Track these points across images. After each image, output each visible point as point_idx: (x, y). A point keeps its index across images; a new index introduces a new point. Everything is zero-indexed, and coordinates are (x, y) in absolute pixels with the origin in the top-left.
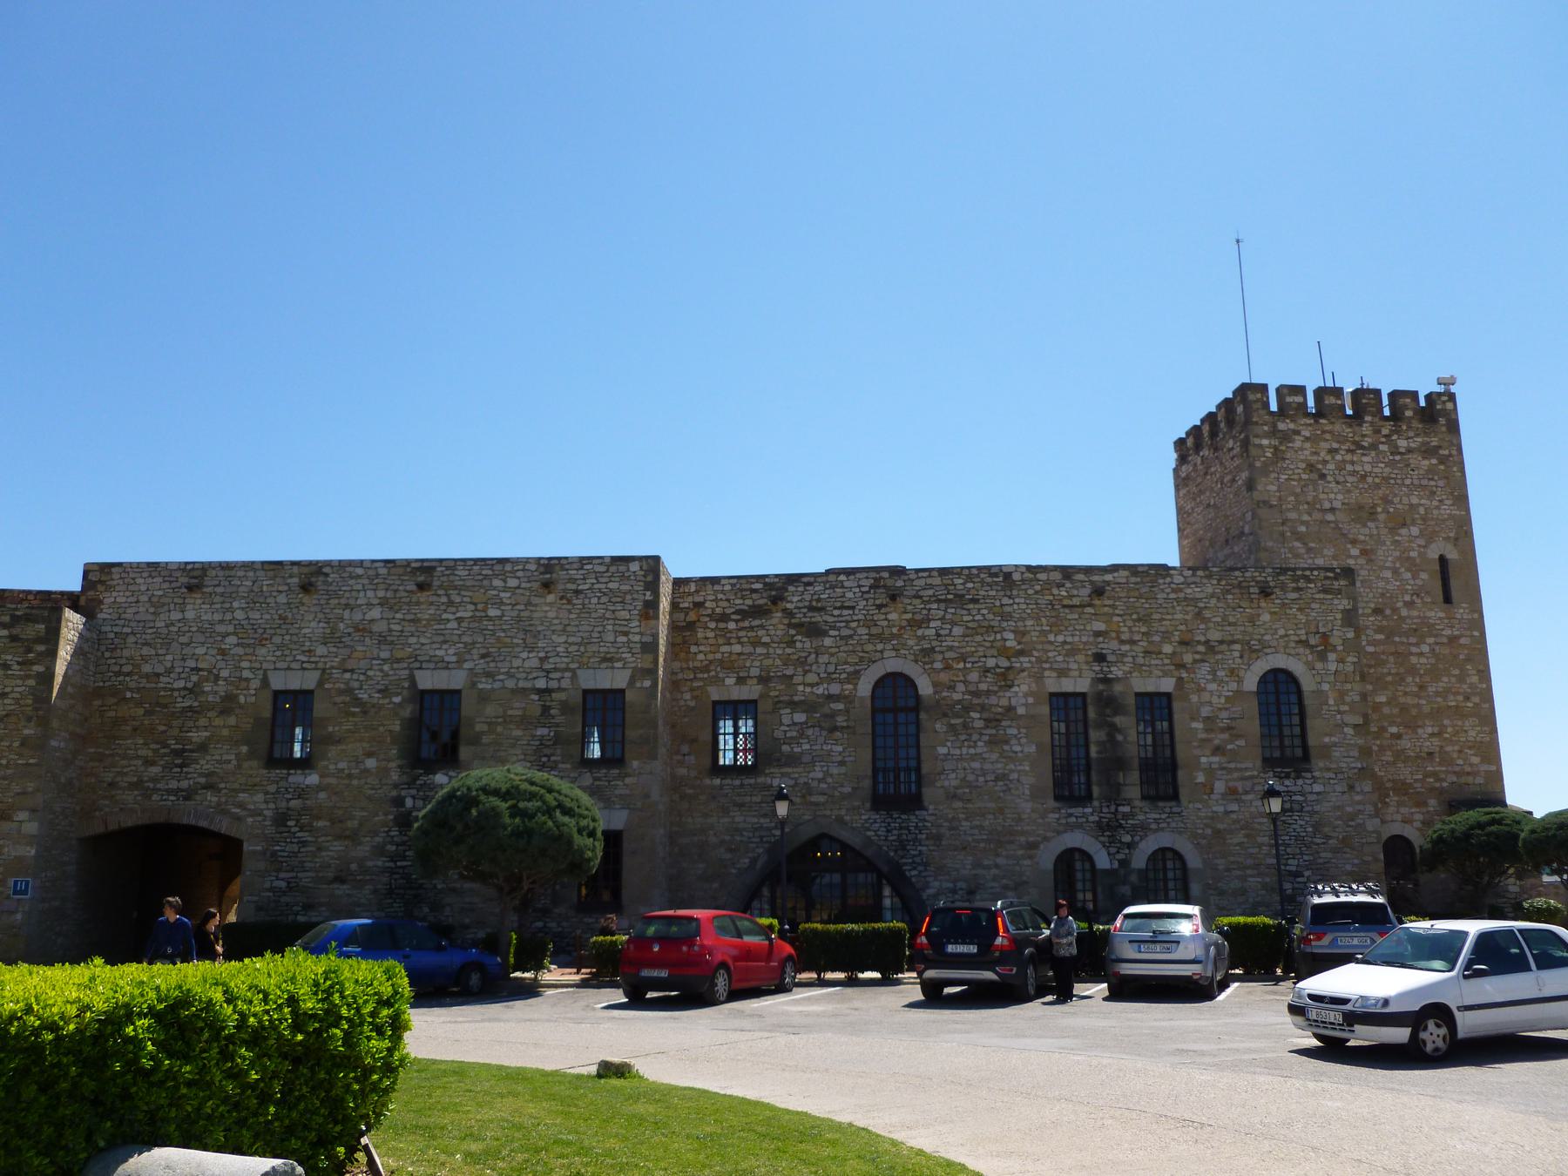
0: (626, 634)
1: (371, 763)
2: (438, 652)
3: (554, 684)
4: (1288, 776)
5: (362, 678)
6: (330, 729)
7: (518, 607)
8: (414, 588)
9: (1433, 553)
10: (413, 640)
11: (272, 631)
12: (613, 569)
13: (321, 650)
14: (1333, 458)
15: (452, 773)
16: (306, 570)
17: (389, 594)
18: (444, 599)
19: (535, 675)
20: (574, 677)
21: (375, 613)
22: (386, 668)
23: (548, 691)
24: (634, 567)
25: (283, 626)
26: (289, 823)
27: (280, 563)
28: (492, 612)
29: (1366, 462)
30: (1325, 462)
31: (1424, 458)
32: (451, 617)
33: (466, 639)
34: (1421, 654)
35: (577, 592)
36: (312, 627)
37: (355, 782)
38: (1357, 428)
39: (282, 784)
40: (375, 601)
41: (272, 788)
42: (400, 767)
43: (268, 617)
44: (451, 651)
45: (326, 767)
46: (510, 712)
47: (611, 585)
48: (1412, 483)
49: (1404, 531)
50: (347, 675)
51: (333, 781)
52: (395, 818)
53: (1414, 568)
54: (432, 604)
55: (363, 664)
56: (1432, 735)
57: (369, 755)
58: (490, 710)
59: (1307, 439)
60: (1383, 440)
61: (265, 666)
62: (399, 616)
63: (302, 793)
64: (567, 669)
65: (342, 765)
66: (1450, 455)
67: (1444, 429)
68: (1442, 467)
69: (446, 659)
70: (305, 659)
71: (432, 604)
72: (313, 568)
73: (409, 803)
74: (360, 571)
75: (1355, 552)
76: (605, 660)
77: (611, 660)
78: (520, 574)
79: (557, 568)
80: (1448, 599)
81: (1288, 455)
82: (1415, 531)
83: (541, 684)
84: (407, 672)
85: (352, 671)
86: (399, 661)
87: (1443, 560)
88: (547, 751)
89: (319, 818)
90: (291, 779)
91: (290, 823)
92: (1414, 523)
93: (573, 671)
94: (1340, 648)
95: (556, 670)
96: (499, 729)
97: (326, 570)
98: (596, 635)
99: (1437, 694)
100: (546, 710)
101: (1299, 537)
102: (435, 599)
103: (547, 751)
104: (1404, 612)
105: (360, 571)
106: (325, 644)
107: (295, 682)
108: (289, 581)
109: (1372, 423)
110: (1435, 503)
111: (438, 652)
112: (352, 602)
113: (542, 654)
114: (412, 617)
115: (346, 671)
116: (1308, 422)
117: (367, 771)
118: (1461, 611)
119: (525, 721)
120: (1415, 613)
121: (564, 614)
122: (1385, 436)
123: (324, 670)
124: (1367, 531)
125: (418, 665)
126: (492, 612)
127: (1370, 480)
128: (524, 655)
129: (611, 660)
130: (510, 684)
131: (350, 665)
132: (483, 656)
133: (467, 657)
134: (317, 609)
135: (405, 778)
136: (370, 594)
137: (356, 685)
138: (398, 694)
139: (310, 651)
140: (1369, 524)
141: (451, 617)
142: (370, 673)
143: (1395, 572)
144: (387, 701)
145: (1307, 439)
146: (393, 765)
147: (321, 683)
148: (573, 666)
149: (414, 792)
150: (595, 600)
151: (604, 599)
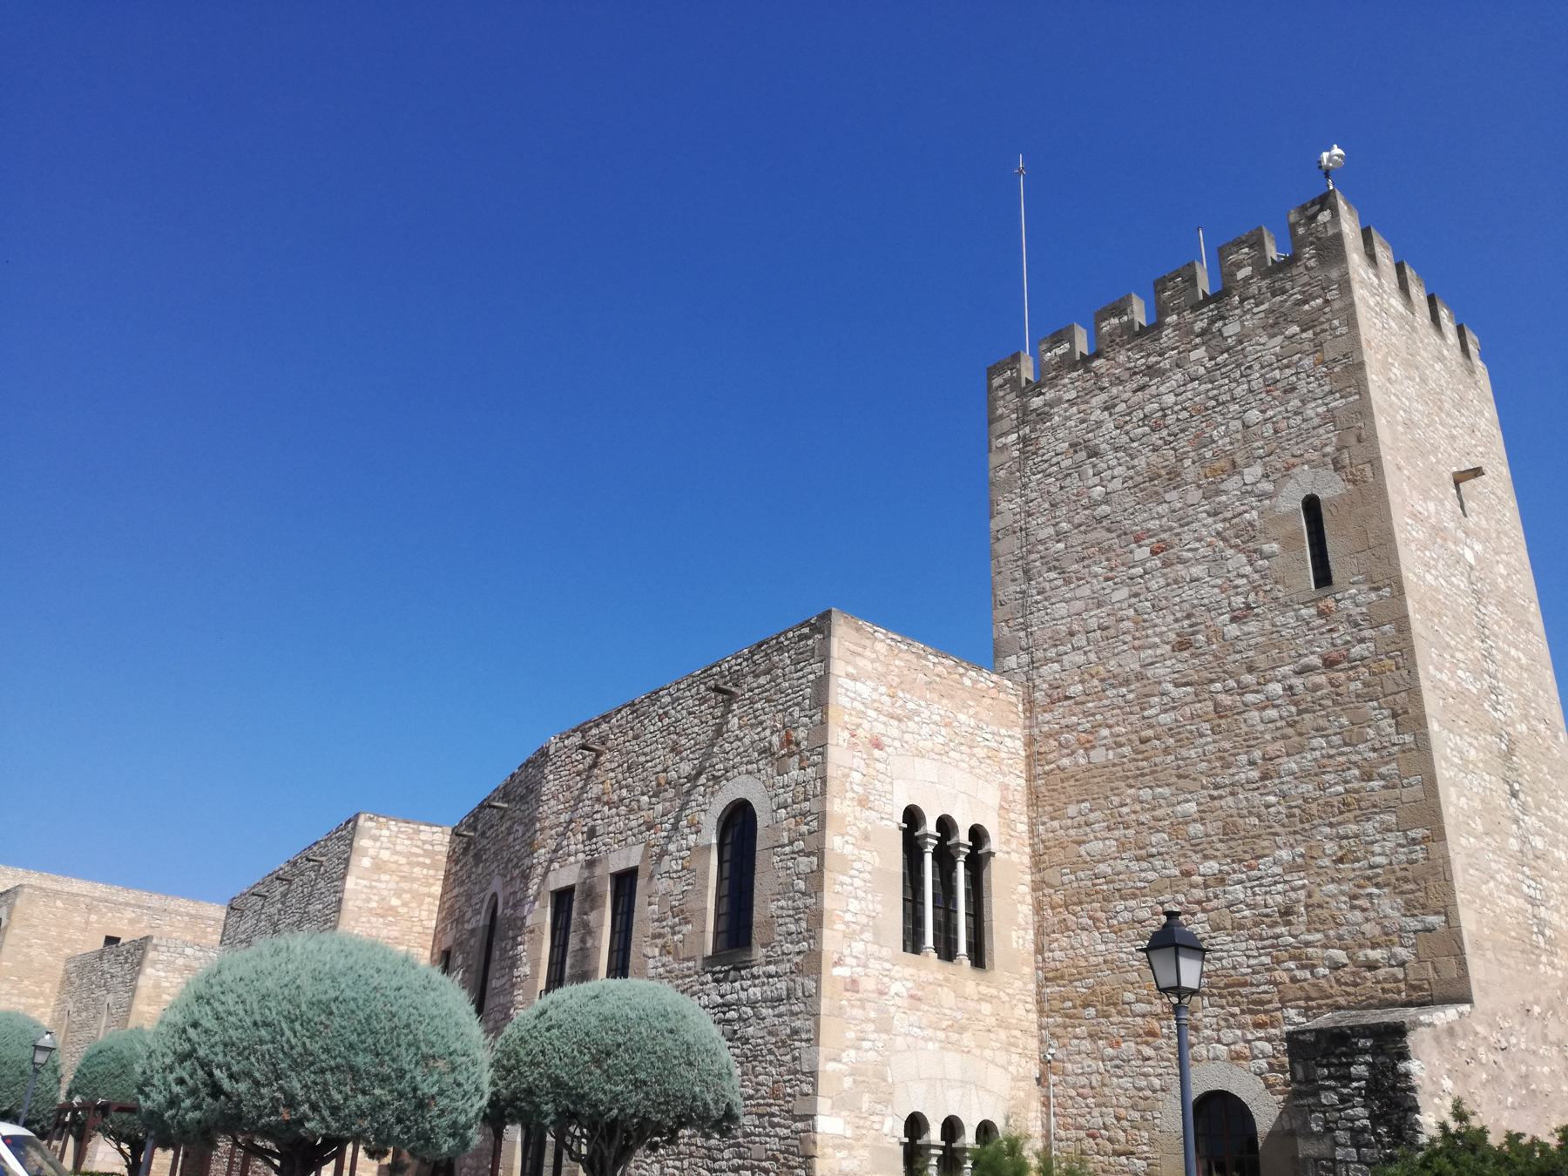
4: (725, 979)
9: (1290, 502)
14: (1111, 415)
29: (1166, 393)
30: (1099, 424)
31: (1272, 336)
34: (1270, 702)
38: (1151, 347)
48: (1250, 391)
49: (1232, 484)
53: (1246, 538)
56: (1292, 868)
59: (1072, 403)
60: (1198, 340)
66: (1327, 302)
67: (1312, 263)
68: (1309, 334)
75: (1142, 553)
80: (1323, 577)
81: (1043, 441)
82: (1253, 473)
87: (1312, 506)
92: (1251, 460)
94: (804, 745)
99: (1303, 775)
101: (1054, 564)
104: (1233, 630)
109: (1177, 327)
110: (1295, 403)
116: (1075, 374)
118: (1352, 595)
120: (1252, 626)
122: (1203, 333)
124: (1165, 507)
127: (1171, 419)
140: (1167, 497)
143: (1218, 560)
145: (1072, 403)
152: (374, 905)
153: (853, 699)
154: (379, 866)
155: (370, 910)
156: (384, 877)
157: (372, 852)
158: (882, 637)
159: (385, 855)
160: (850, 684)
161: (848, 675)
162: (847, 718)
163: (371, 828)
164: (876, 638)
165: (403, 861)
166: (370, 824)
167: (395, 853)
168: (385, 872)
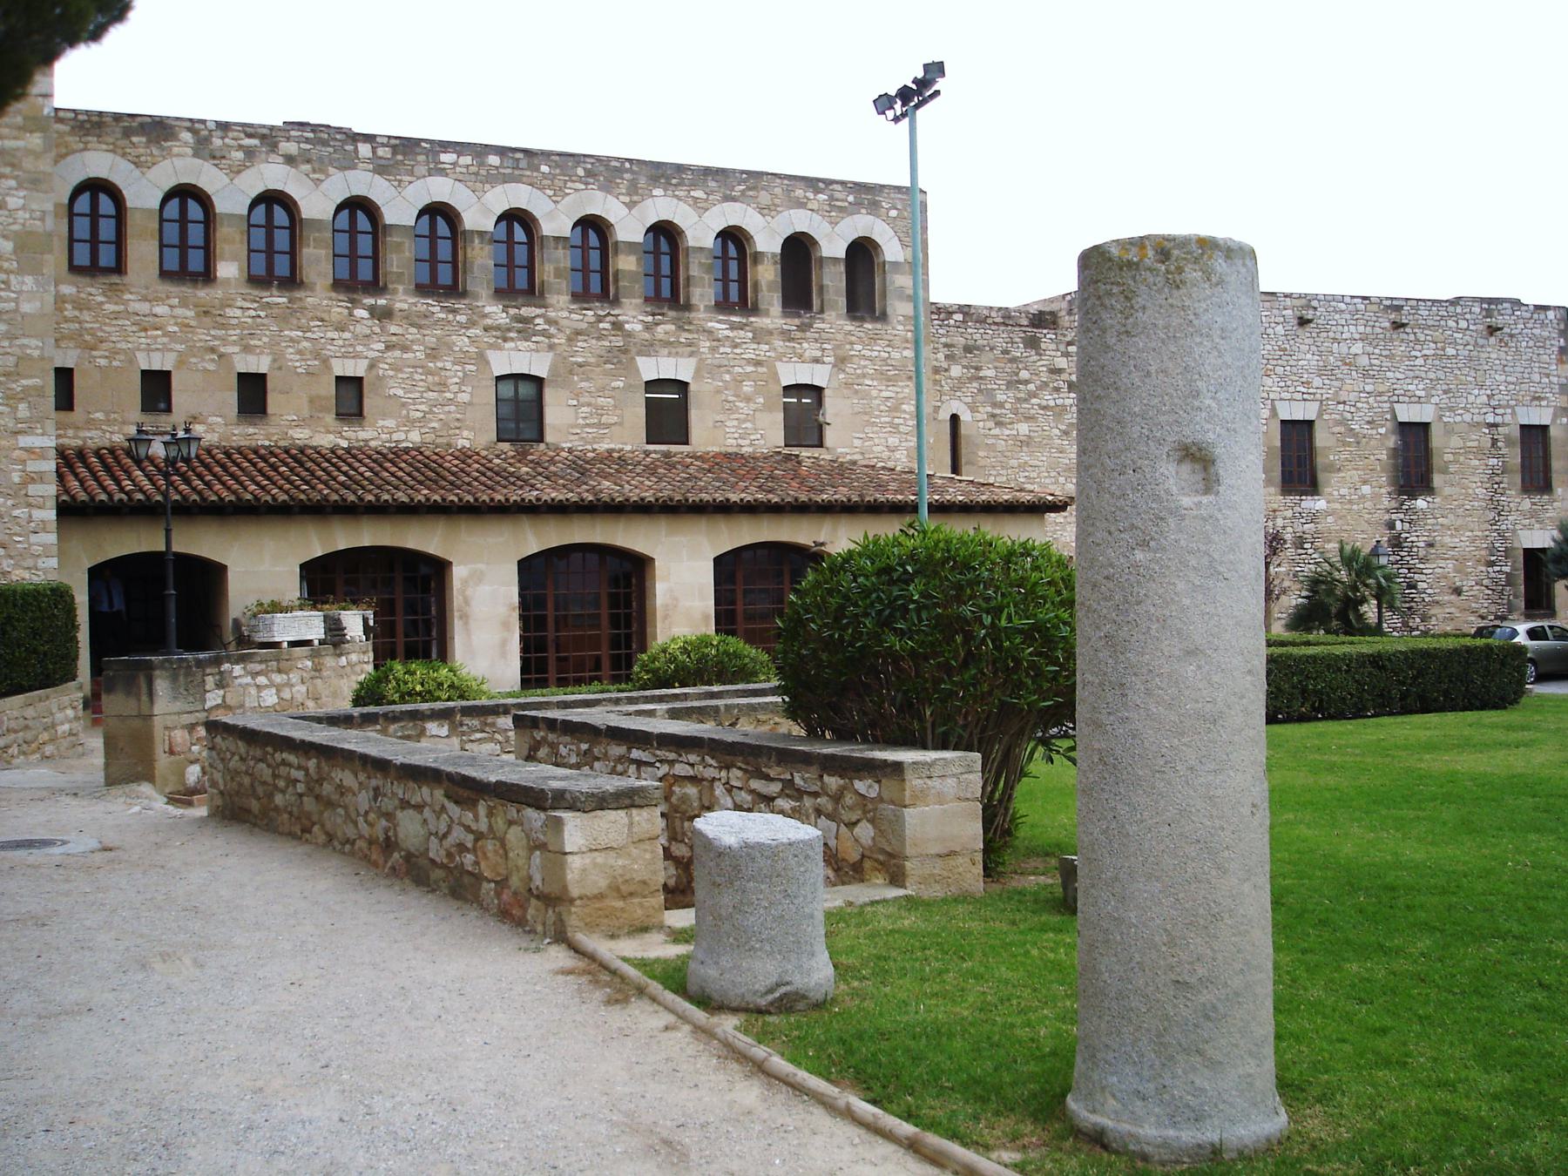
0: (1548, 376)
1: (1366, 489)
2: (1410, 387)
3: (1499, 419)
5: (1353, 409)
6: (1332, 457)
7: (1468, 347)
8: (1387, 325)
10: (1389, 374)
11: (1275, 362)
12: (1536, 316)
13: (1317, 382)
15: (1429, 499)
16: (1298, 303)
17: (1369, 330)
18: (1412, 337)
19: (1484, 410)
20: (1514, 414)
21: (1357, 348)
22: (1371, 400)
23: (1495, 425)
24: (1551, 314)
25: (1284, 358)
26: (1306, 546)
27: (1273, 294)
28: (1451, 351)
32: (1418, 354)
33: (1432, 375)
35: (1512, 336)
36: (1310, 360)
37: (1355, 507)
39: (1297, 509)
40: (1357, 336)
41: (1289, 513)
42: (1389, 493)
43: (1269, 347)
44: (1421, 387)
45: (1331, 494)
46: (1469, 444)
47: (1534, 331)
50: (1341, 407)
51: (1337, 506)
52: (1389, 541)
54: (1402, 341)
55: (1352, 397)
57: (1365, 482)
58: (1455, 442)
61: (1272, 396)
62: (1377, 351)
63: (1314, 517)
64: (1508, 406)
65: (1343, 492)
69: (1418, 393)
70: (1305, 390)
71: (1402, 341)
72: (1303, 302)
73: (1398, 525)
74: (1342, 306)
76: (1535, 398)
77: (1539, 399)
78: (1468, 316)
79: (1496, 313)
83: (1490, 419)
84: (1388, 405)
85: (1344, 403)
86: (1381, 394)
88: (1497, 479)
89: (1329, 541)
90: (1304, 504)
91: (1306, 546)
93: (1512, 407)
95: (1500, 406)
96: (1462, 459)
97: (1315, 303)
98: (1526, 376)
100: (1494, 442)
102: (1405, 336)
103: (1497, 479)
105: (1342, 306)
106: (1319, 376)
107: (1298, 413)
108: (1284, 312)
111: (1410, 387)
112: (1338, 336)
113: (1489, 392)
114: (1387, 353)
115: (1339, 403)
117: (1363, 496)
119: (1479, 452)
121: (1503, 355)
123: (1321, 401)
125: (1395, 398)
126: (1451, 351)
128: (1476, 392)
129: (1539, 399)
130: (1467, 417)
131: (1343, 396)
132: (1445, 392)
133: (1434, 392)
134: (1310, 341)
135: (1394, 504)
136: (1352, 328)
137: (1349, 416)
138: (1382, 426)
139: (1308, 383)
141: (1418, 354)
142: (1359, 405)
144: (1374, 432)
146: (1383, 491)
147: (1320, 414)
148: (1513, 403)
149: (1402, 516)
150: (1524, 344)
151: (1531, 343)
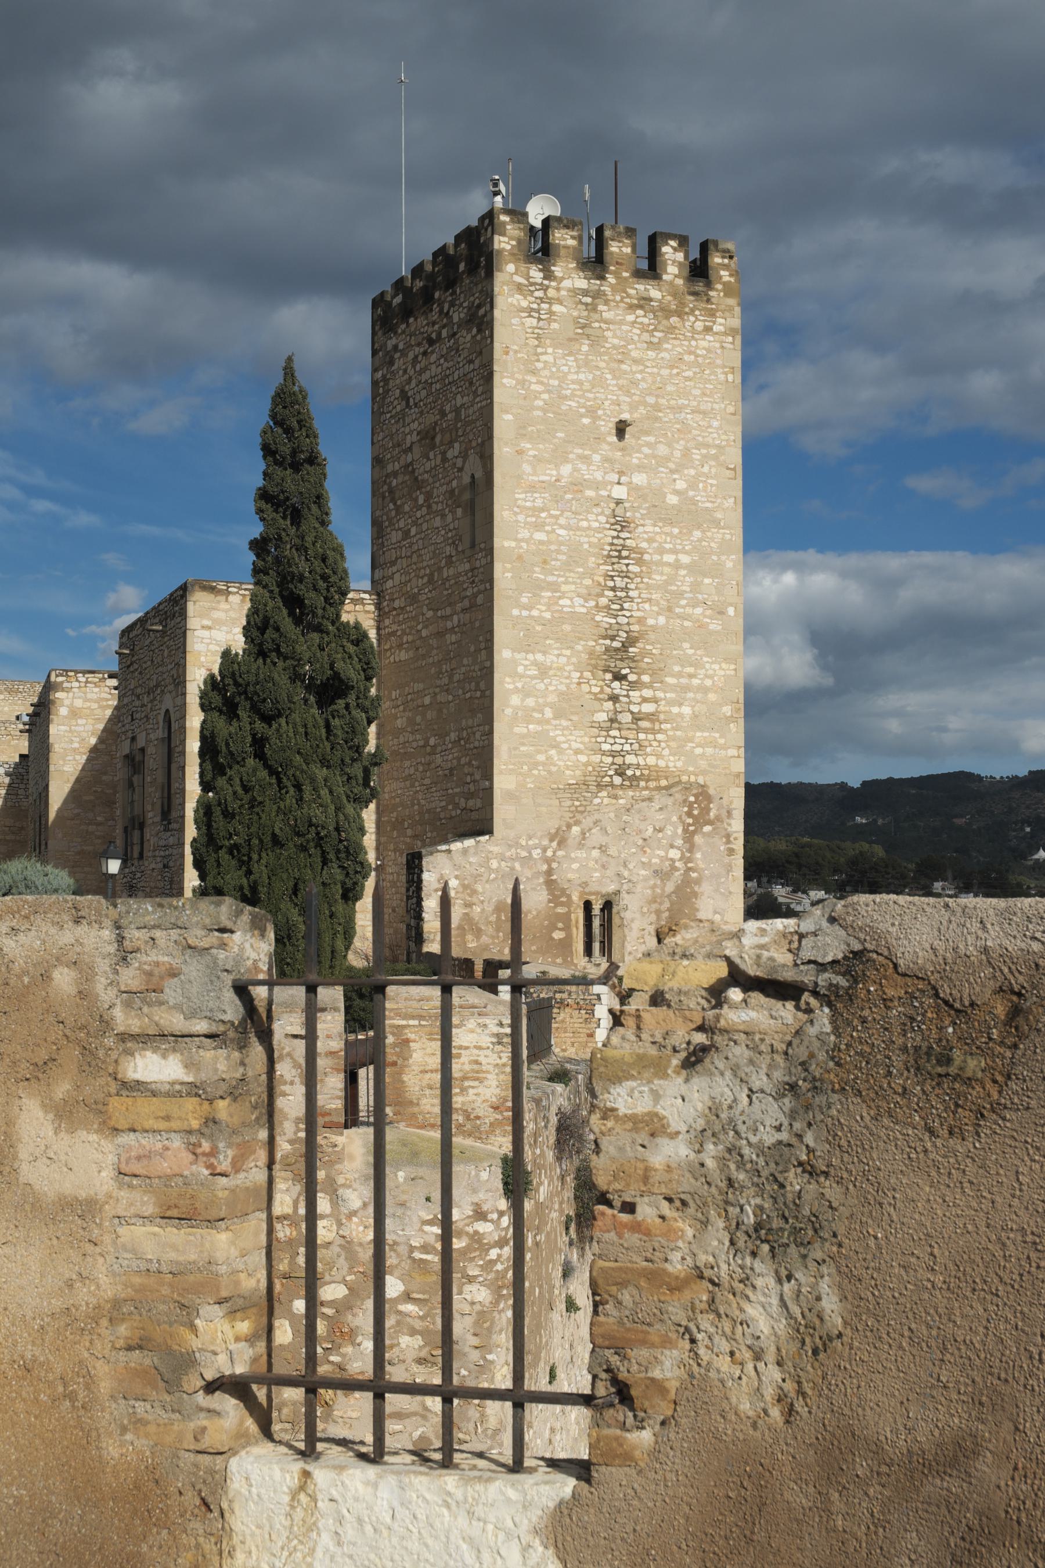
152: (76, 745)
153: (208, 644)
154: (74, 713)
155: (75, 750)
156: (80, 721)
157: (67, 702)
158: (235, 590)
159: (79, 703)
160: (206, 633)
161: (203, 627)
162: (203, 659)
163: (62, 682)
164: (230, 593)
165: (95, 706)
166: (60, 679)
167: (86, 700)
168: (80, 717)
